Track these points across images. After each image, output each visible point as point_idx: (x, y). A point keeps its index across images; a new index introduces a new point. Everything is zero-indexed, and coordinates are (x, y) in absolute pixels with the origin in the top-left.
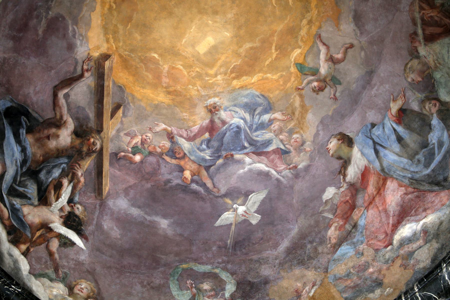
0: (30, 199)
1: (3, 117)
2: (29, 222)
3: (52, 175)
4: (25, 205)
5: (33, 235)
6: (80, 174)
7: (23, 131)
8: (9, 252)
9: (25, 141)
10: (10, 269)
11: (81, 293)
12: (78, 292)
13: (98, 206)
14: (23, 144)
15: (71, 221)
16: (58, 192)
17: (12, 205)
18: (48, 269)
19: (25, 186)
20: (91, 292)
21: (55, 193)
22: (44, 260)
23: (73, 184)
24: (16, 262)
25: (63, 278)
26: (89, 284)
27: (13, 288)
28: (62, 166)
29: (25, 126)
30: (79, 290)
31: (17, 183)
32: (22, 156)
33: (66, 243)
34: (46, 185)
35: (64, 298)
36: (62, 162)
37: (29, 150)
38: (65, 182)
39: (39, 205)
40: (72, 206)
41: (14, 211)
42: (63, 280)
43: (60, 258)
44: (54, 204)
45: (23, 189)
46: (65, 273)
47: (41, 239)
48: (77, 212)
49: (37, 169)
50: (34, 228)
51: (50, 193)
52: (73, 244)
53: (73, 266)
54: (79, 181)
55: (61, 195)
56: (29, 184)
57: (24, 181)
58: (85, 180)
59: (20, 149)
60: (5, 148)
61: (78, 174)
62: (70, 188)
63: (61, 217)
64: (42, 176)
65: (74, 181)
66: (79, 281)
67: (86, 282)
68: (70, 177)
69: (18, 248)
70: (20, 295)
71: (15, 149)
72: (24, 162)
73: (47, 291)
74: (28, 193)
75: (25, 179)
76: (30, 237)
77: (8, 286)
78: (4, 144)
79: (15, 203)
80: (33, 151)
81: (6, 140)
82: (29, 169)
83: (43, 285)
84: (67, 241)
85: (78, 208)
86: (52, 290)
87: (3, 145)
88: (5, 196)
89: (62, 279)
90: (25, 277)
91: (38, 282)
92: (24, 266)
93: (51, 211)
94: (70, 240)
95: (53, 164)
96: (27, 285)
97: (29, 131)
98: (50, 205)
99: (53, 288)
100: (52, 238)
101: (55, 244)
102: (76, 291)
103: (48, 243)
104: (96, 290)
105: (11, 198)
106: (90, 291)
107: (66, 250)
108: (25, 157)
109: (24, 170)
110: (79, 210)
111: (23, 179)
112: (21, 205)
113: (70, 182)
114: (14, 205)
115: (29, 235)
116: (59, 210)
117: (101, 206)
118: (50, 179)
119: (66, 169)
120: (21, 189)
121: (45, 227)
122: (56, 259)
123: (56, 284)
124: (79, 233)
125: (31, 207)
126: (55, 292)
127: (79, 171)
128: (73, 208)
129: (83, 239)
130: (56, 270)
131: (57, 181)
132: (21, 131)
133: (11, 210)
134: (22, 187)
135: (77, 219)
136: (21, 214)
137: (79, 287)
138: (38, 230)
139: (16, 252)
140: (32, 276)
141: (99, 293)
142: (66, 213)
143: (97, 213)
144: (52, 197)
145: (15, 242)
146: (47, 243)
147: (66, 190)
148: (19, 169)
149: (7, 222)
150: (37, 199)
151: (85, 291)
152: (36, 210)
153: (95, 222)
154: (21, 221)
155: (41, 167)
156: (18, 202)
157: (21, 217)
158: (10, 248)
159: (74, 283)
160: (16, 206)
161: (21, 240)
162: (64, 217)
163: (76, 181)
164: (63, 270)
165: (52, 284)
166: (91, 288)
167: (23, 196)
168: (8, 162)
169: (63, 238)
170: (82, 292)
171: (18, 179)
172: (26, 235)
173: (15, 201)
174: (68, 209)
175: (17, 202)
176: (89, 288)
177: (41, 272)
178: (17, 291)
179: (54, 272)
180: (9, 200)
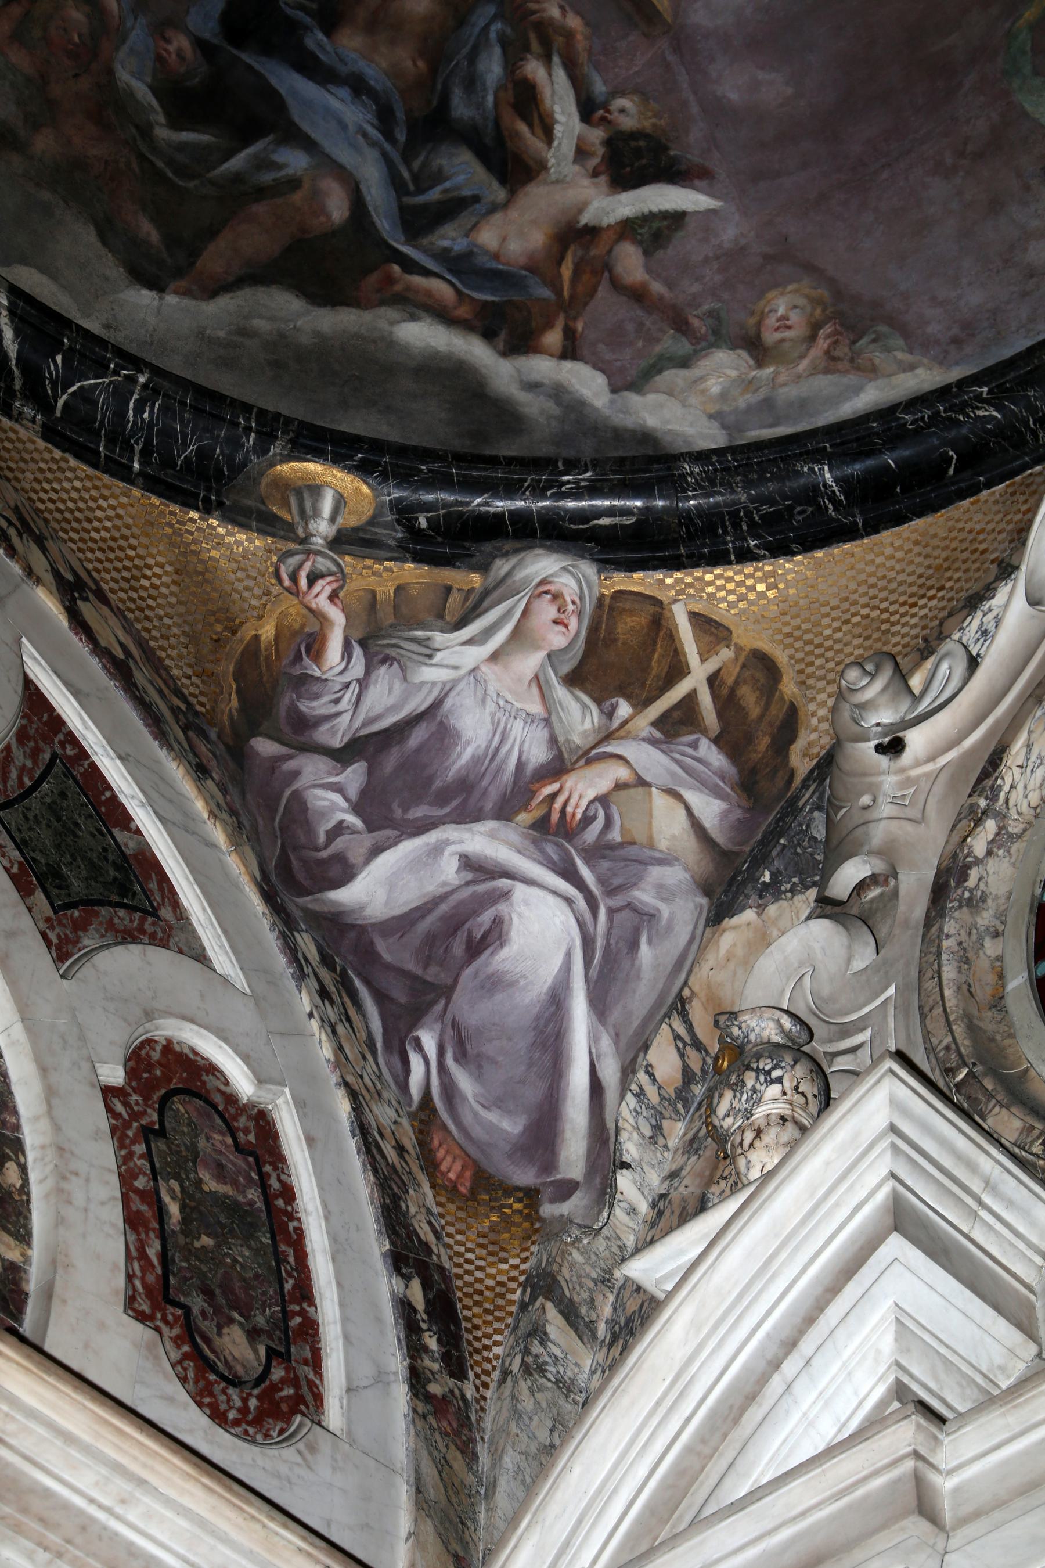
0: (476, 199)
1: (235, 52)
2: (522, 260)
3: (484, 84)
4: (475, 226)
5: (555, 285)
6: (555, 12)
7: (315, 39)
8: (521, 381)
9: (341, 60)
10: (554, 423)
11: (788, 334)
12: (778, 336)
13: (671, 58)
14: (343, 70)
15: (631, 161)
16: (536, 115)
17: (444, 256)
18: (658, 340)
19: (439, 177)
20: (814, 309)
21: (531, 126)
22: (630, 327)
23: (561, 56)
24: (558, 392)
25: (716, 332)
26: (796, 291)
27: (568, 482)
28: (493, 35)
29: (308, 20)
30: (777, 329)
31: (412, 188)
32: (365, 106)
33: (656, 232)
34: (491, 125)
35: (750, 382)
36: (482, 23)
37: (374, 73)
38: (534, 69)
39: (513, 193)
40: (603, 119)
41: (461, 266)
42: (720, 335)
43: (670, 285)
44: (550, 154)
45: (438, 189)
46: (713, 314)
47: (585, 277)
48: (628, 123)
49: (435, 103)
50: (541, 266)
51: (517, 134)
52: (677, 219)
53: (718, 278)
54: (569, 35)
55: (551, 115)
56: (444, 162)
57: (424, 165)
58: (583, 17)
59: (344, 92)
60: (306, 127)
61: (551, 19)
62: (560, 75)
63: (595, 174)
64: (461, 109)
65: (555, 46)
66: (762, 303)
67: (782, 294)
68: (535, 45)
69: (540, 352)
70: (599, 484)
71: (335, 104)
72: (385, 118)
73: (693, 400)
74: (458, 188)
75: (422, 158)
76: (553, 297)
77: (552, 487)
78: (296, 119)
79: (446, 243)
80: (384, 65)
81: (289, 101)
82: (412, 127)
83: (670, 394)
84: (656, 225)
85: (622, 111)
86: (702, 387)
87: (293, 124)
88: (405, 249)
89: (712, 339)
90: (607, 412)
91: (651, 398)
92: (588, 383)
93: (557, 181)
94: (665, 215)
95: (465, 51)
96: (626, 430)
97: (330, 23)
98: (542, 166)
99: (702, 379)
100: (610, 251)
101: (631, 263)
102: (770, 337)
103: (610, 271)
104: (824, 293)
105: (425, 241)
106: (809, 309)
107: (670, 251)
108: (377, 104)
109: (401, 136)
110: (628, 113)
111: (416, 164)
112: (467, 235)
113: (547, 59)
114: (446, 250)
115: (546, 293)
116: (575, 161)
117: (677, 49)
118: (490, 99)
119: (509, 31)
120: (434, 195)
121: (573, 234)
122: (661, 298)
123: (703, 363)
124: (674, 173)
125: (498, 217)
126: (714, 386)
127: (546, 5)
128: (609, 122)
129: (697, 182)
130: (681, 325)
131: (510, 86)
132: (309, 43)
133: (450, 271)
134: (431, 187)
135: (642, 143)
136: (486, 258)
137: (771, 321)
138: (560, 260)
139: (542, 367)
140: (626, 394)
141: (838, 293)
142: (601, 151)
143: (683, 78)
144: (530, 139)
145: (520, 342)
146: (606, 274)
147: (553, 92)
148: (388, 147)
149: (463, 312)
150: (495, 185)
151: (795, 317)
152: (513, 214)
153: (695, 109)
154: (498, 277)
155: (439, 87)
156: (453, 234)
157: (488, 265)
158: (518, 371)
159: (752, 321)
160: (456, 248)
161: (533, 324)
162: (603, 168)
163: (559, 41)
164: (699, 312)
165: (695, 372)
166: (807, 296)
167: (453, 208)
168: (344, 156)
169: (641, 227)
170: (789, 327)
171: (406, 175)
172: (538, 299)
173: (444, 237)
174: (596, 135)
175: (449, 237)
176: (801, 301)
177: (643, 364)
178: (584, 480)
179: (678, 335)
180: (425, 251)
